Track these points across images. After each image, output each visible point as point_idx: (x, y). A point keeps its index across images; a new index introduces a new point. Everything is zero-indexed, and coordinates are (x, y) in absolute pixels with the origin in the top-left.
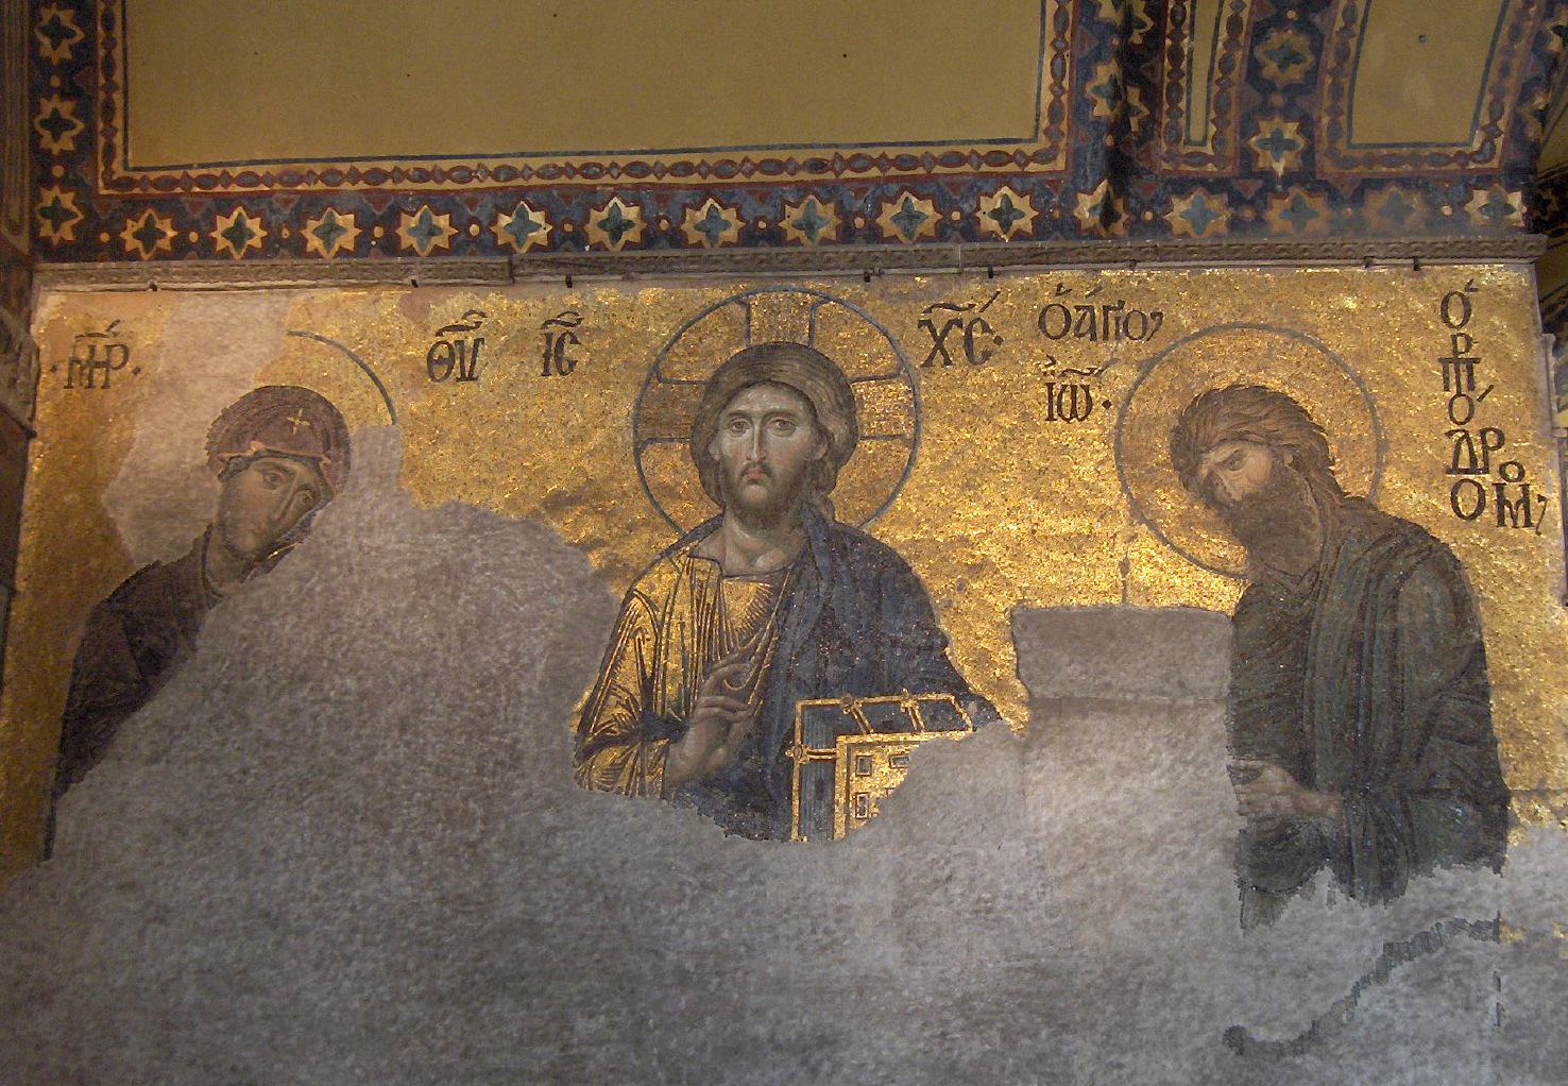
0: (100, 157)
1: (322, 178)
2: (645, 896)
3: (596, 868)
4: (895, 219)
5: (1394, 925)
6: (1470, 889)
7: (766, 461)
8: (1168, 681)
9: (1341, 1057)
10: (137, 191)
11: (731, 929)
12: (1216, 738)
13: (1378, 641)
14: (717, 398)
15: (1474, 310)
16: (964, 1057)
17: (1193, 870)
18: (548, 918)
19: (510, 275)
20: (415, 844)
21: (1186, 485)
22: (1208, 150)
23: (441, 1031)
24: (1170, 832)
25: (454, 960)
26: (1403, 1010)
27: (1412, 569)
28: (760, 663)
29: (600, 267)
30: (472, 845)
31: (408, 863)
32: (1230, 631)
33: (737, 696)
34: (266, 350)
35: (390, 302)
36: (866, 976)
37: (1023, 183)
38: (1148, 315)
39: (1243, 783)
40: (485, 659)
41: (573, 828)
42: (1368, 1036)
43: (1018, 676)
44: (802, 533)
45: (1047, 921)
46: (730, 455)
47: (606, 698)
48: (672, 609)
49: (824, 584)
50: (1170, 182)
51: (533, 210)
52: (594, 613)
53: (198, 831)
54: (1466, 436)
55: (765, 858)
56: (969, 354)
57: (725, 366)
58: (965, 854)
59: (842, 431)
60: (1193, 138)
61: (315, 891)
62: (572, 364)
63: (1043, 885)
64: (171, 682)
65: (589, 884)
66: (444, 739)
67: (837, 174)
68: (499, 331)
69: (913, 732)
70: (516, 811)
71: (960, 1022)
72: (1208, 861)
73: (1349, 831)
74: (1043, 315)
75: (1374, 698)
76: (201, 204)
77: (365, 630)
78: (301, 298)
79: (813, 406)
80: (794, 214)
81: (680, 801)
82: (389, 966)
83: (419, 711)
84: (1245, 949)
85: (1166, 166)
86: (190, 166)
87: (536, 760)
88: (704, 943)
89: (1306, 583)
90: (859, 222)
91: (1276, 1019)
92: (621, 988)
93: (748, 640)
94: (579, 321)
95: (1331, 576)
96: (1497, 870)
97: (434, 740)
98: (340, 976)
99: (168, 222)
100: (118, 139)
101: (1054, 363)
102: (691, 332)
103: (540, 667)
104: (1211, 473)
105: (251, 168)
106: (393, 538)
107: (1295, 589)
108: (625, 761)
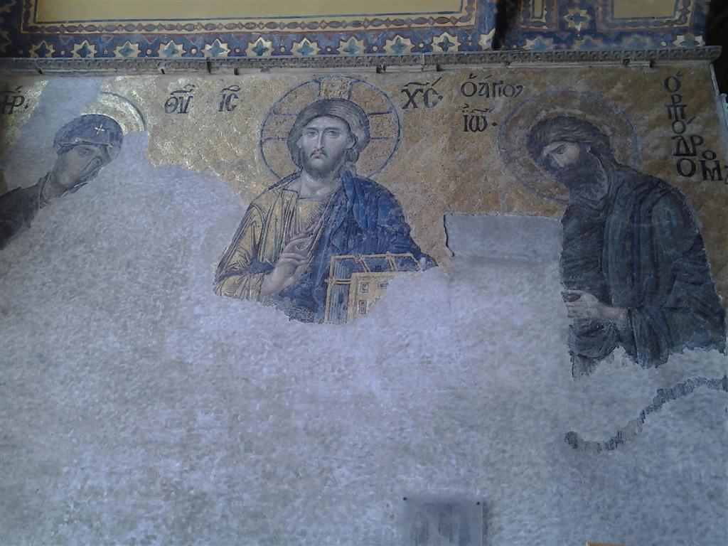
0: (23, 16)
1: (125, 28)
2: (243, 350)
3: (218, 335)
4: (393, 47)
5: (662, 379)
6: (706, 361)
8: (527, 250)
9: (636, 452)
10: (39, 32)
11: (288, 368)
12: (554, 278)
13: (642, 233)
14: (302, 121)
15: (682, 83)
16: (413, 443)
17: (544, 345)
18: (190, 361)
19: (209, 66)
20: (126, 322)
21: (535, 160)
22: (544, 20)
23: (123, 418)
24: (530, 325)
25: (136, 382)
26: (672, 427)
27: (659, 199)
29: (250, 63)
30: (155, 323)
31: (120, 332)
32: (561, 227)
33: (300, 253)
34: (89, 99)
35: (150, 80)
36: (359, 396)
37: (454, 31)
38: (515, 87)
39: (571, 301)
40: (175, 234)
41: (209, 315)
42: (652, 442)
43: (447, 245)
45: (461, 369)
47: (234, 254)
49: (348, 202)
50: (526, 33)
51: (222, 43)
53: (13, 313)
54: (683, 139)
55: (309, 332)
56: (426, 103)
57: (305, 109)
58: (417, 332)
60: (536, 15)
61: (69, 344)
62: (234, 107)
63: (460, 350)
64: (15, 241)
65: (214, 343)
66: (149, 271)
67: (366, 27)
68: (201, 93)
69: (391, 271)
70: (181, 306)
71: (412, 422)
72: (552, 341)
73: (632, 328)
74: (463, 86)
75: (642, 261)
76: (68, 38)
77: (117, 221)
78: (109, 79)
80: (344, 45)
81: (267, 303)
82: (101, 383)
83: (138, 258)
84: (575, 389)
85: (523, 27)
86: (65, 22)
87: (195, 282)
88: (273, 375)
89: (601, 204)
90: (375, 48)
91: (595, 429)
92: (225, 398)
93: (308, 228)
94: (239, 90)
95: (614, 201)
96: (722, 351)
97: (143, 271)
98: (74, 388)
99: (52, 46)
100: (32, 9)
101: (468, 106)
103: (202, 238)
104: (548, 155)
105: (91, 23)
106: (138, 180)
107: (595, 207)
108: (240, 284)
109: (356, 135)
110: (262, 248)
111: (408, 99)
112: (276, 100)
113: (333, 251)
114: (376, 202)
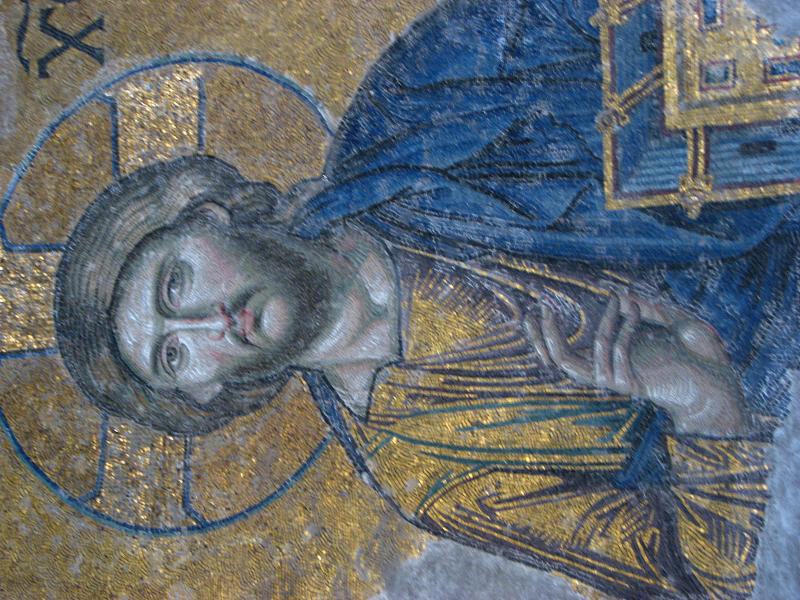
7: (228, 305)
14: (129, 396)
28: (541, 281)
33: (595, 324)
44: (338, 231)
46: (215, 366)
47: (594, 556)
48: (451, 447)
52: (453, 586)
57: (86, 388)
59: (190, 182)
79: (150, 236)
81: (775, 405)
102: (30, 448)
108: (707, 515)
109: (183, 202)
110: (576, 459)
111: (73, 53)
112: (49, 503)
113: (584, 209)
114: (416, 93)
